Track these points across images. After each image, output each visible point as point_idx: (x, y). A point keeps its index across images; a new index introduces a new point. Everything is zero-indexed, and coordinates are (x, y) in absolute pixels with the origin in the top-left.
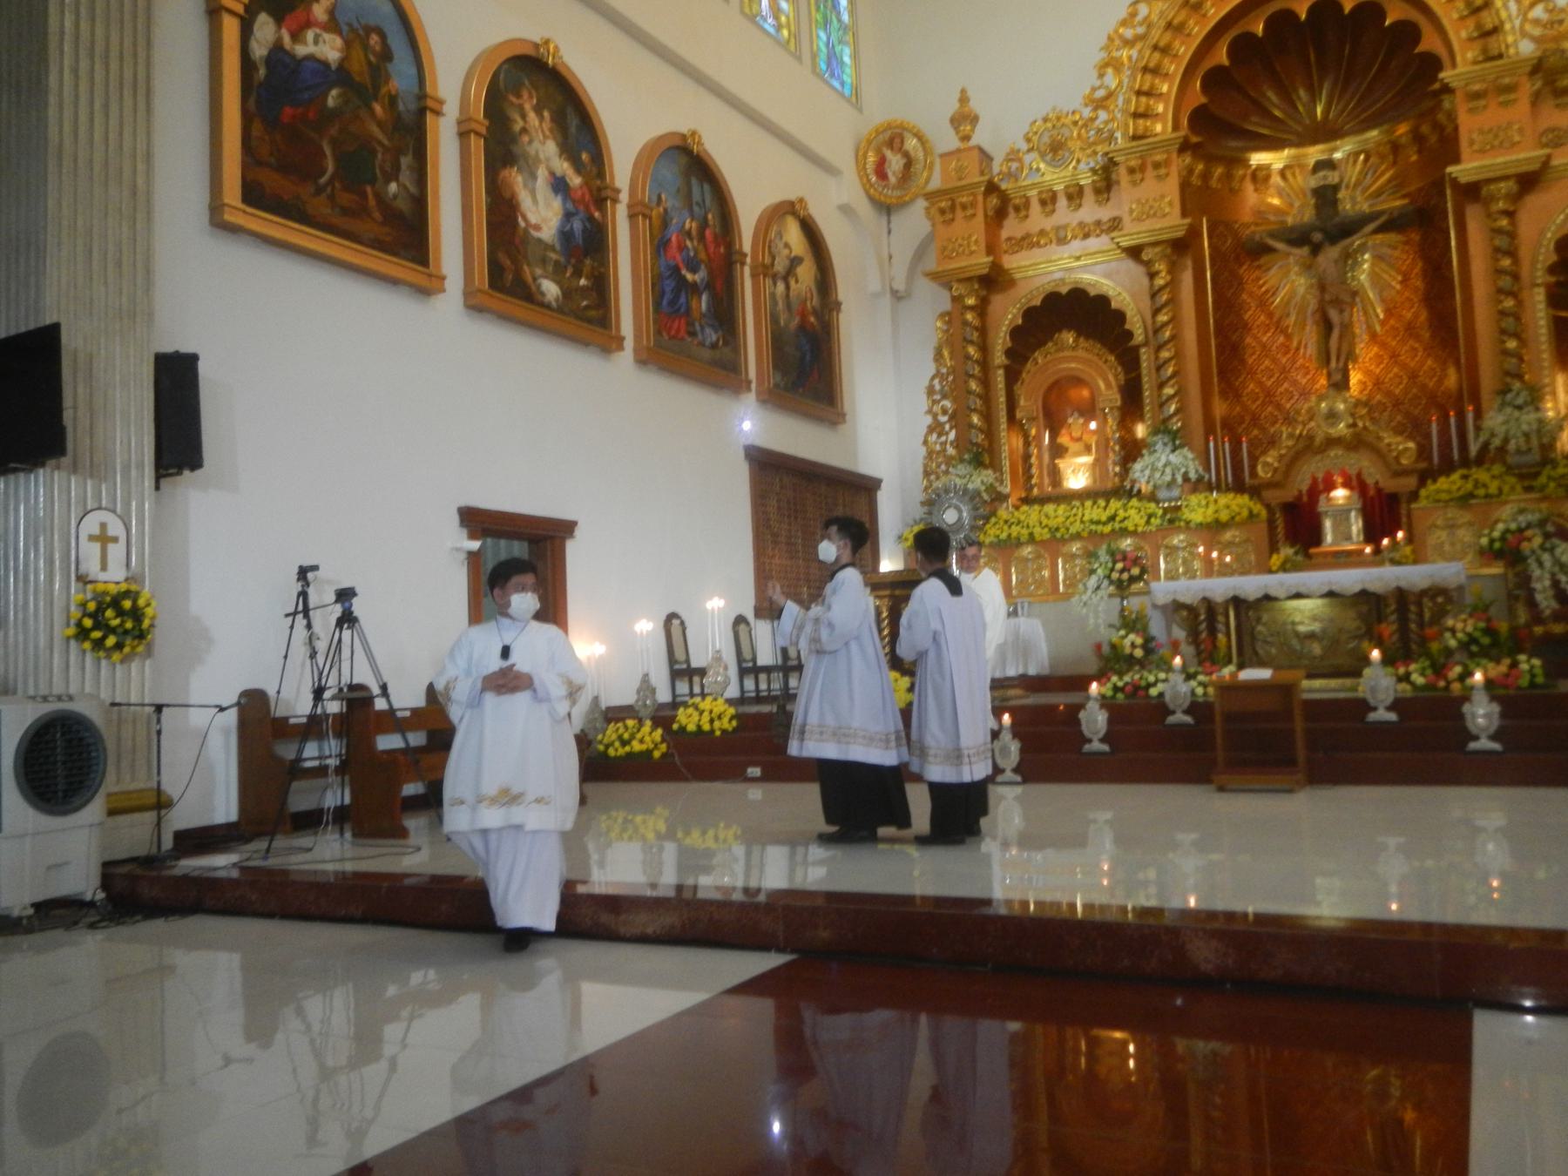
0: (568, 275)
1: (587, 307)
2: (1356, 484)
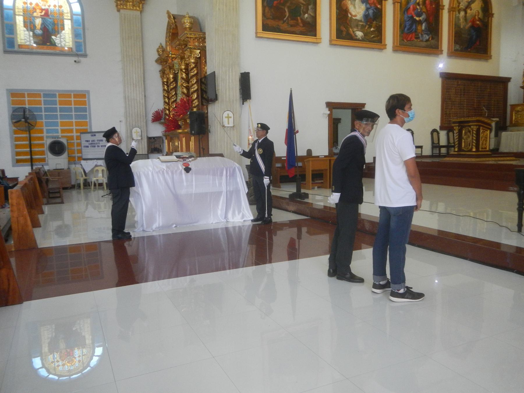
0: (366, 28)
1: (374, 37)
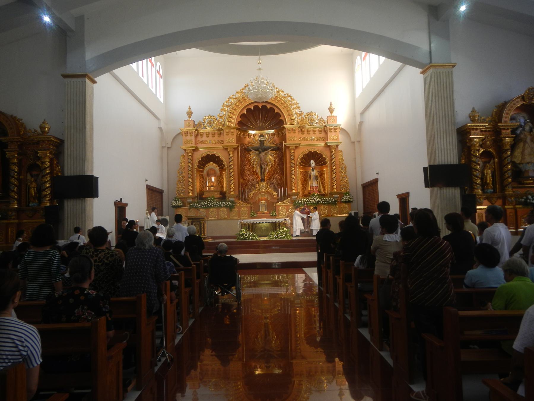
2: (266, 200)
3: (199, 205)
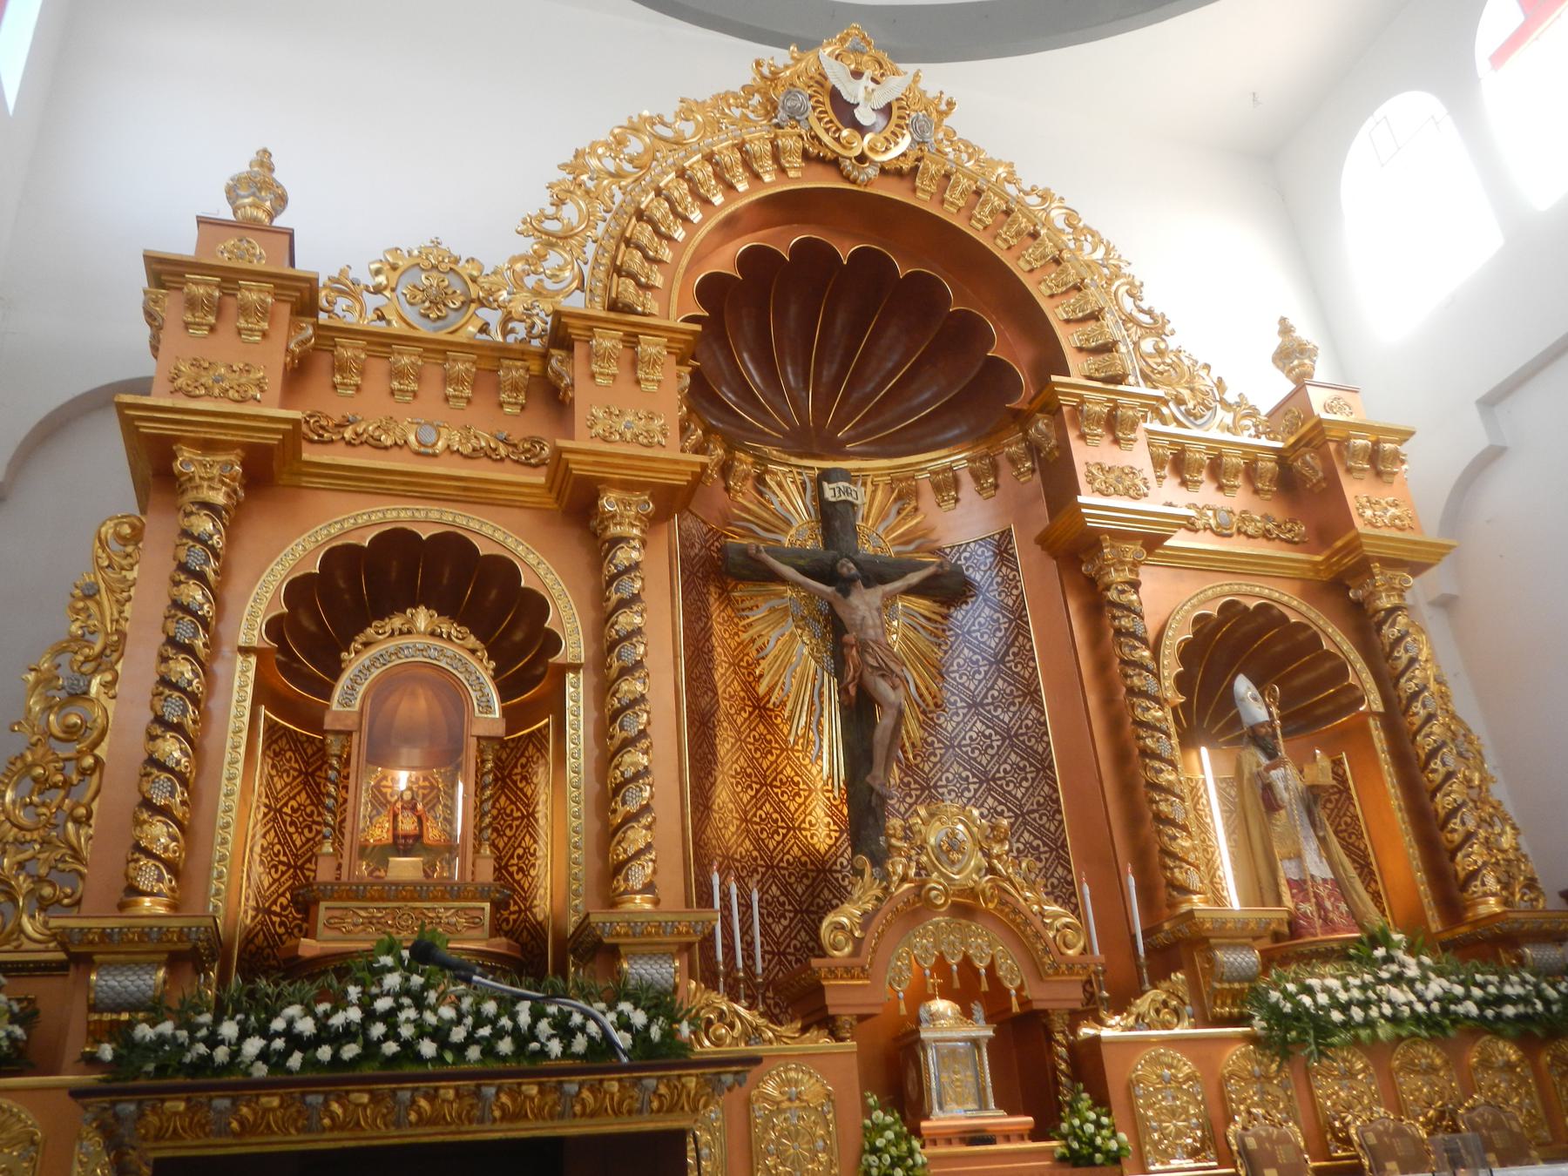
3: (244, 1034)
